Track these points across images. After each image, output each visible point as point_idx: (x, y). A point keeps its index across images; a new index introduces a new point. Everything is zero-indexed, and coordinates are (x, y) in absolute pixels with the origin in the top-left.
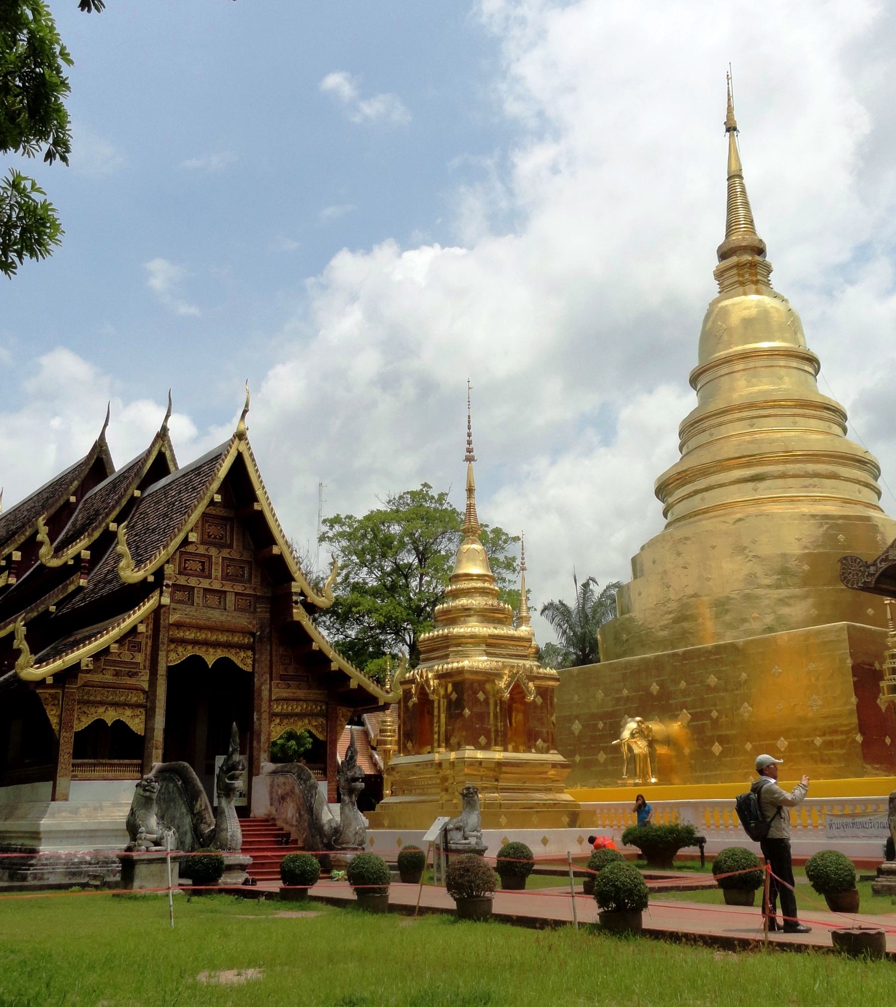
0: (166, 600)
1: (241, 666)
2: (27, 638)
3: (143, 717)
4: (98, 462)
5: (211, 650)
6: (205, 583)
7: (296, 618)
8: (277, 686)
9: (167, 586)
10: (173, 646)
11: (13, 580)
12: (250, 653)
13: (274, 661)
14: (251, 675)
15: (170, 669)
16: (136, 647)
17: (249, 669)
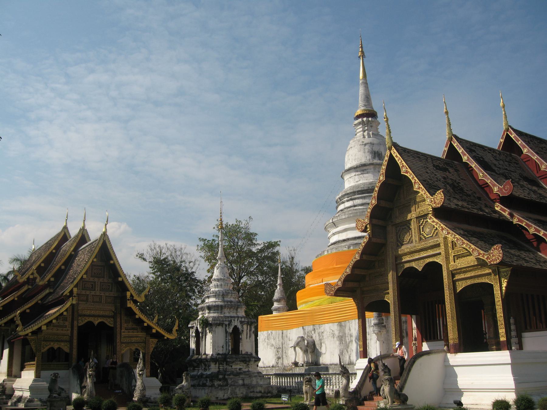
0: (74, 302)
1: (108, 324)
2: (21, 319)
3: (69, 346)
4: (64, 236)
5: (96, 319)
6: (93, 293)
7: (129, 305)
8: (124, 332)
9: (75, 296)
10: (80, 318)
11: (30, 287)
12: (112, 319)
15: (79, 328)
16: (65, 319)
17: (112, 326)
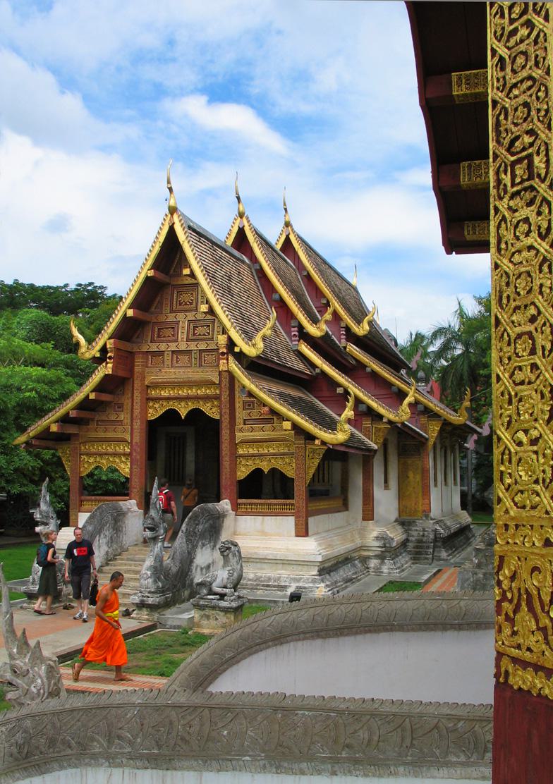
5: (183, 404)
8: (241, 430)
9: (110, 358)
13: (237, 405)
14: (217, 421)
16: (121, 406)
17: (217, 417)
